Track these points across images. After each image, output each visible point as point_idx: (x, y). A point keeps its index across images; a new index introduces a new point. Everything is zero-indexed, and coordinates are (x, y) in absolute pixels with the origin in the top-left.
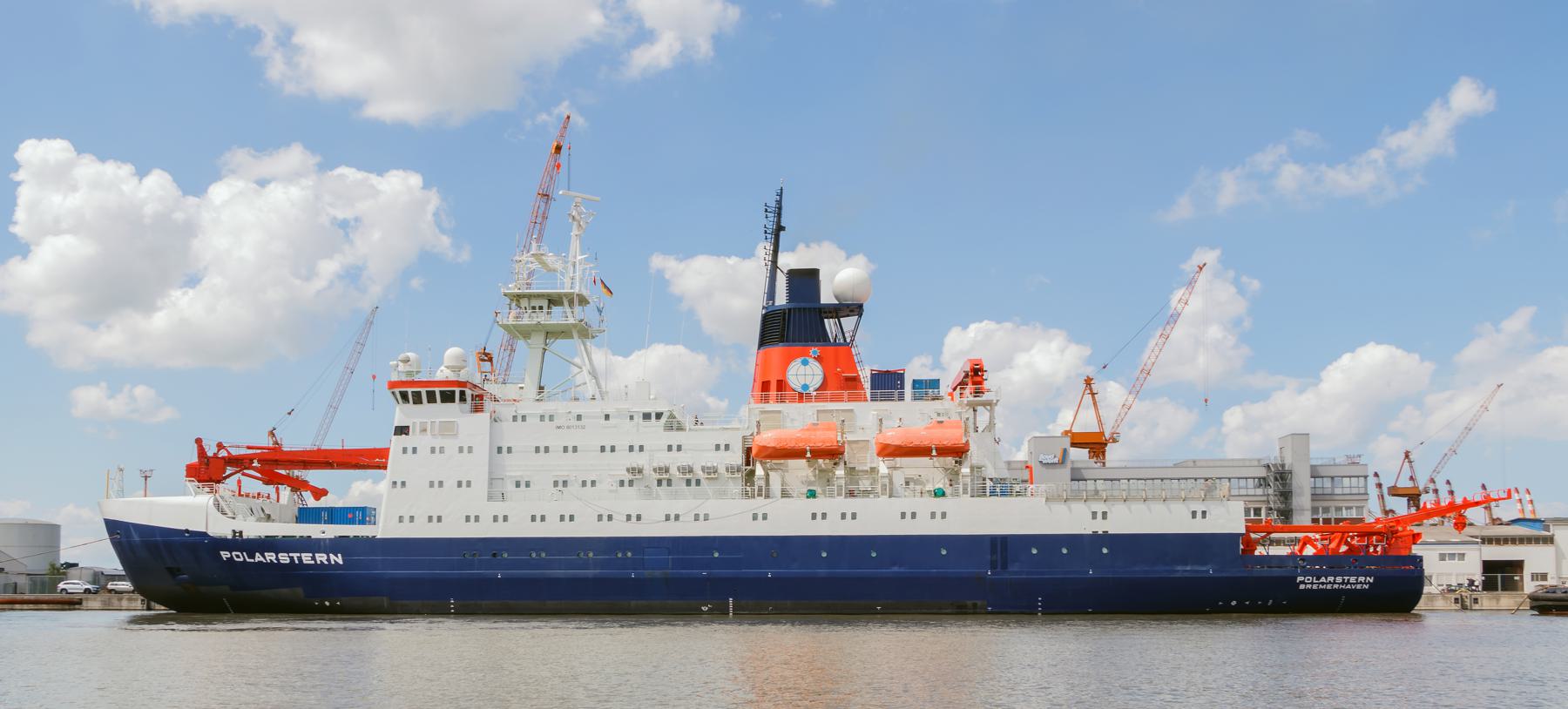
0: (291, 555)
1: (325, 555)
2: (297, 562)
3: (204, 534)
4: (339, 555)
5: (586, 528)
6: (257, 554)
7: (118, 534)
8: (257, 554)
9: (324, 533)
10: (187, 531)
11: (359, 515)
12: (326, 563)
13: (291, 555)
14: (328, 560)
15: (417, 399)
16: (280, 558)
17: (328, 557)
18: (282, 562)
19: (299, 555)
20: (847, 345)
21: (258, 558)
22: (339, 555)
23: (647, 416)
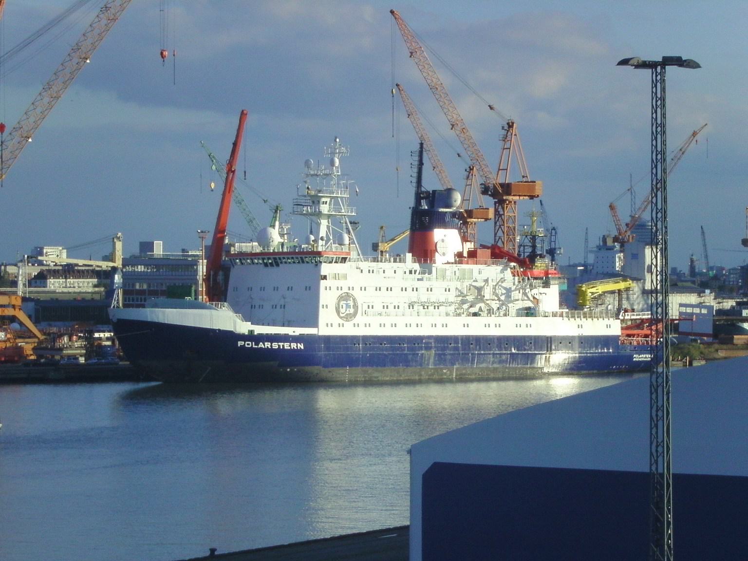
0: (279, 344)
1: (295, 344)
6: (261, 343)
8: (261, 343)
12: (270, 347)
13: (279, 344)
14: (297, 347)
16: (277, 346)
17: (297, 345)
18: (273, 347)
19: (283, 344)
21: (261, 345)
22: (302, 344)
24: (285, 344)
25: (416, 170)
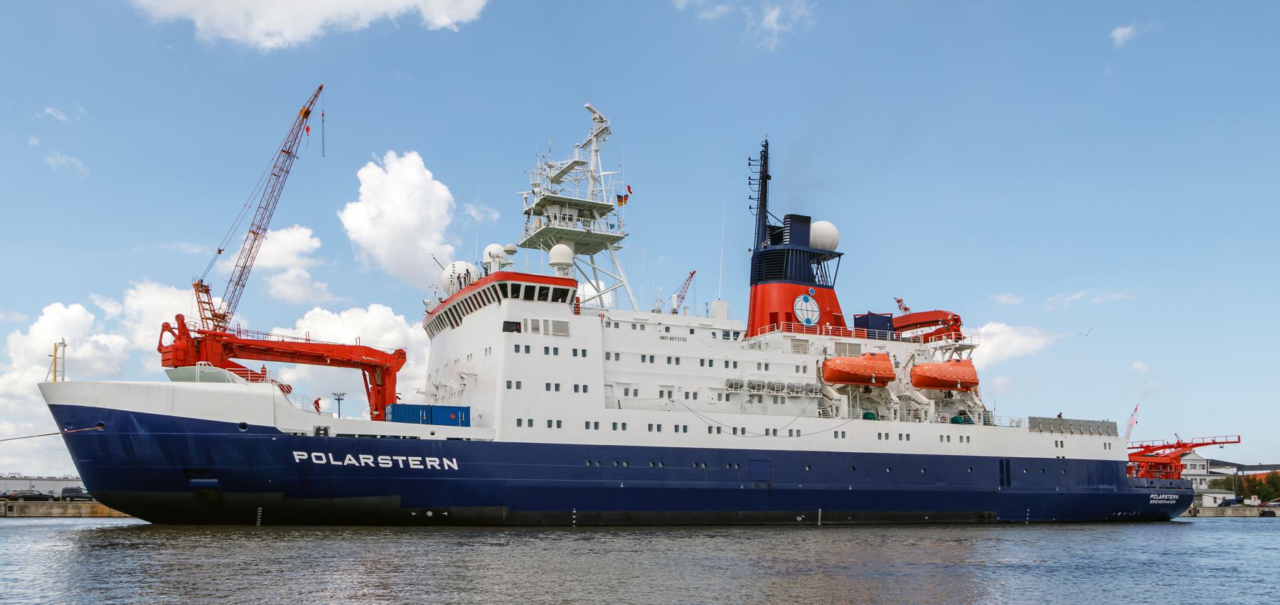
0: (394, 458)
2: (402, 466)
3: (273, 430)
4: (454, 460)
5: (697, 439)
6: (349, 456)
7: (101, 425)
8: (349, 456)
9: (433, 434)
10: (243, 425)
11: (461, 415)
13: (394, 458)
14: (441, 464)
15: (529, 295)
16: (390, 462)
19: (405, 458)
20: (832, 287)
21: (350, 460)
22: (454, 460)
23: (726, 335)
24: (410, 458)
25: (756, 187)
